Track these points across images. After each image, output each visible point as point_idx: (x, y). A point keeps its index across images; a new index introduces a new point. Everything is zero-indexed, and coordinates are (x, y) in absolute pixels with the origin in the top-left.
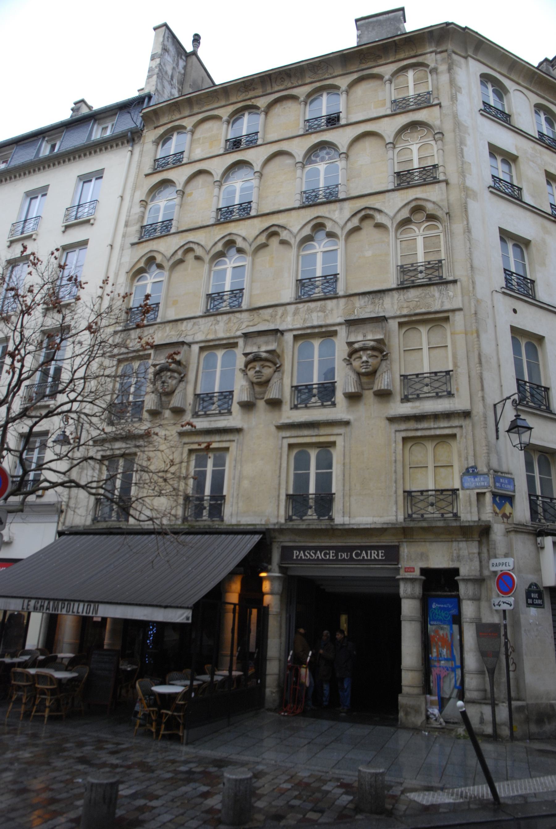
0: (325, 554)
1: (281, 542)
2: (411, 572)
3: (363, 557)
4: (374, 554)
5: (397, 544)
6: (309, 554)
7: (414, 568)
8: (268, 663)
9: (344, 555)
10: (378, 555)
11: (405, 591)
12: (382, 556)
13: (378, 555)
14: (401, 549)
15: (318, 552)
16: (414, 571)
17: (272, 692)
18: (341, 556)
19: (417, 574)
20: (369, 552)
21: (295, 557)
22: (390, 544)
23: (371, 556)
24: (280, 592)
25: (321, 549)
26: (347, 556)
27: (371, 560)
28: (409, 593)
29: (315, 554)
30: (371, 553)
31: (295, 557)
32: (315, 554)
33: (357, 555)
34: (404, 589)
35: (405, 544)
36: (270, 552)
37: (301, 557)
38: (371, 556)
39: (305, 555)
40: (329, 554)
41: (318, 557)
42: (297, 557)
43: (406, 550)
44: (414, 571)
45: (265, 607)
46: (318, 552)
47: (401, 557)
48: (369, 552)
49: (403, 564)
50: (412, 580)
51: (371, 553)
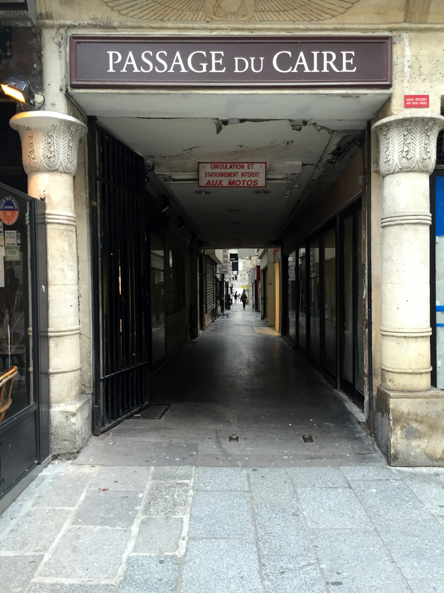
0: (197, 62)
1: (69, 27)
2: (419, 106)
3: (301, 68)
4: (328, 60)
5: (387, 34)
6: (153, 59)
7: (427, 97)
8: (52, 343)
9: (250, 64)
10: (338, 63)
11: (406, 155)
12: (349, 66)
13: (338, 63)
14: (397, 50)
15: (178, 54)
16: (427, 106)
17: (69, 415)
18: (242, 65)
19: (434, 111)
20: (315, 53)
21: (111, 70)
22: (370, 34)
23: (320, 66)
24: (73, 166)
25: (185, 43)
26: (257, 67)
27: (320, 76)
28: (417, 157)
29: (169, 60)
30: (320, 57)
31: (111, 70)
32: (169, 60)
33: (285, 62)
34: (393, 150)
35: (405, 35)
36: (37, 54)
37: (130, 68)
38: (320, 66)
39: (140, 63)
40: (208, 60)
41: (177, 68)
42: (118, 67)
43: (408, 51)
44: (427, 106)
45: (33, 201)
46: (178, 54)
47: (396, 69)
48: (315, 53)
49: (401, 88)
50: (425, 123)
51: (320, 57)
